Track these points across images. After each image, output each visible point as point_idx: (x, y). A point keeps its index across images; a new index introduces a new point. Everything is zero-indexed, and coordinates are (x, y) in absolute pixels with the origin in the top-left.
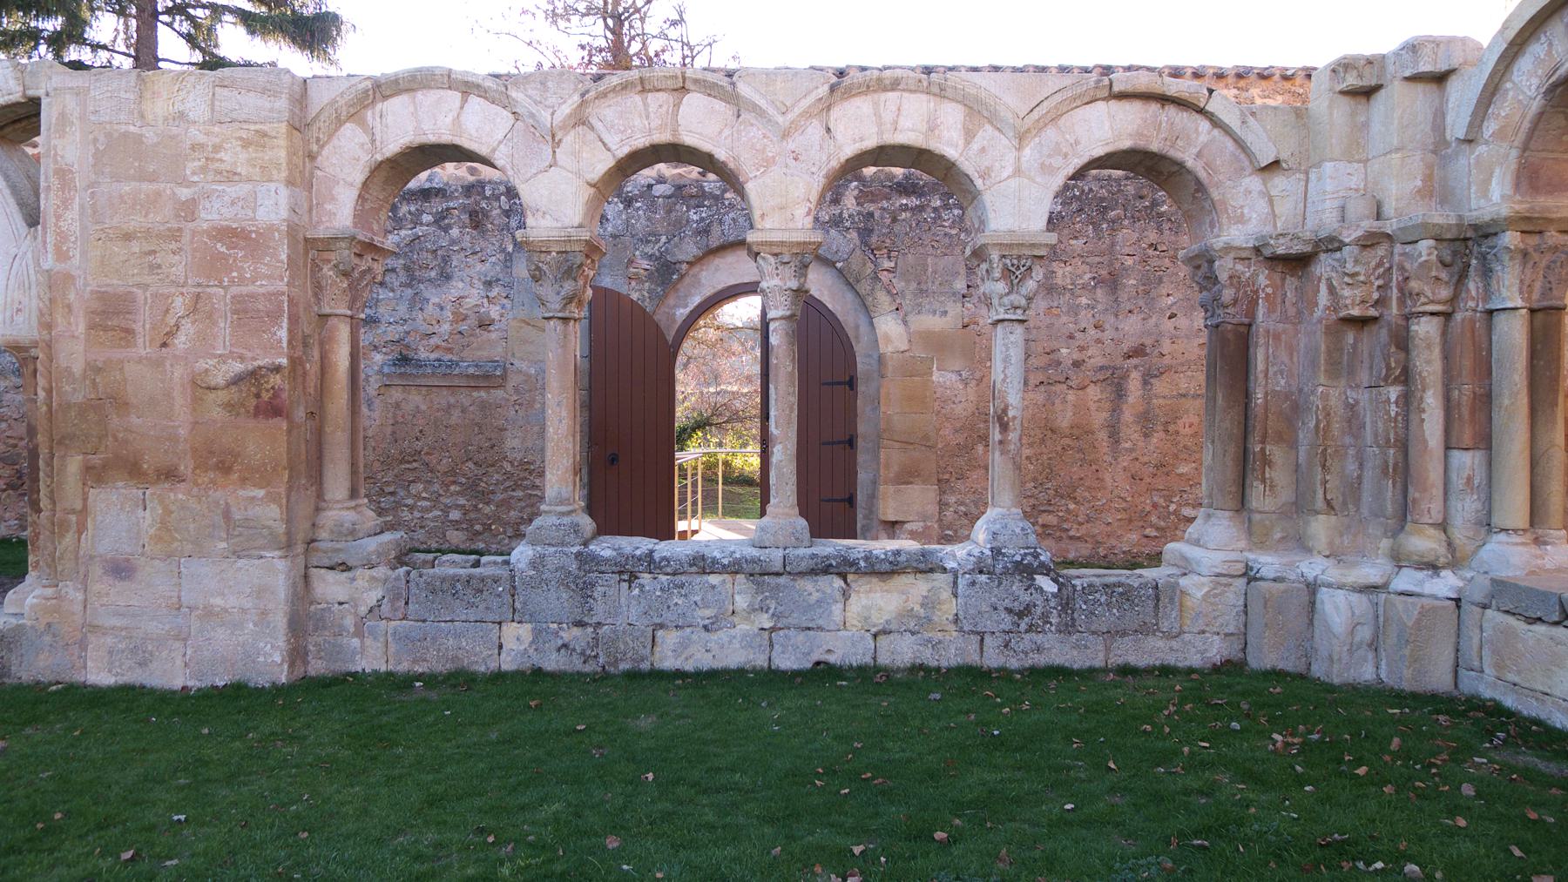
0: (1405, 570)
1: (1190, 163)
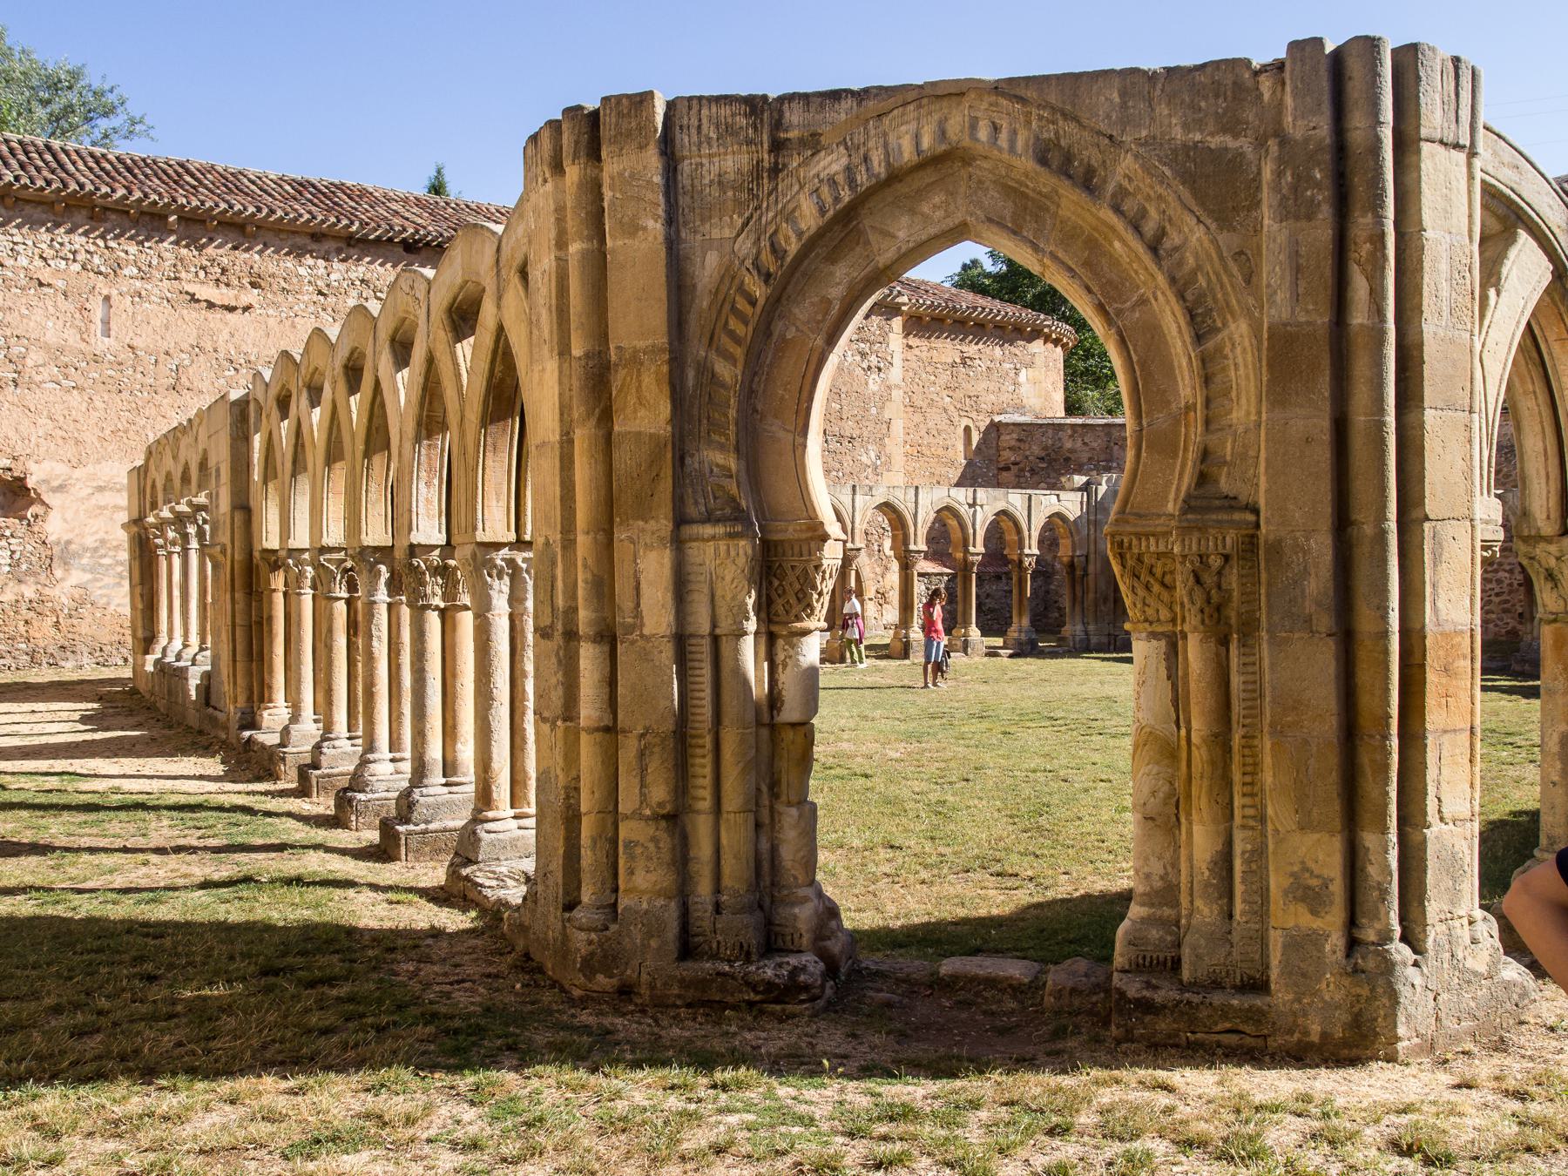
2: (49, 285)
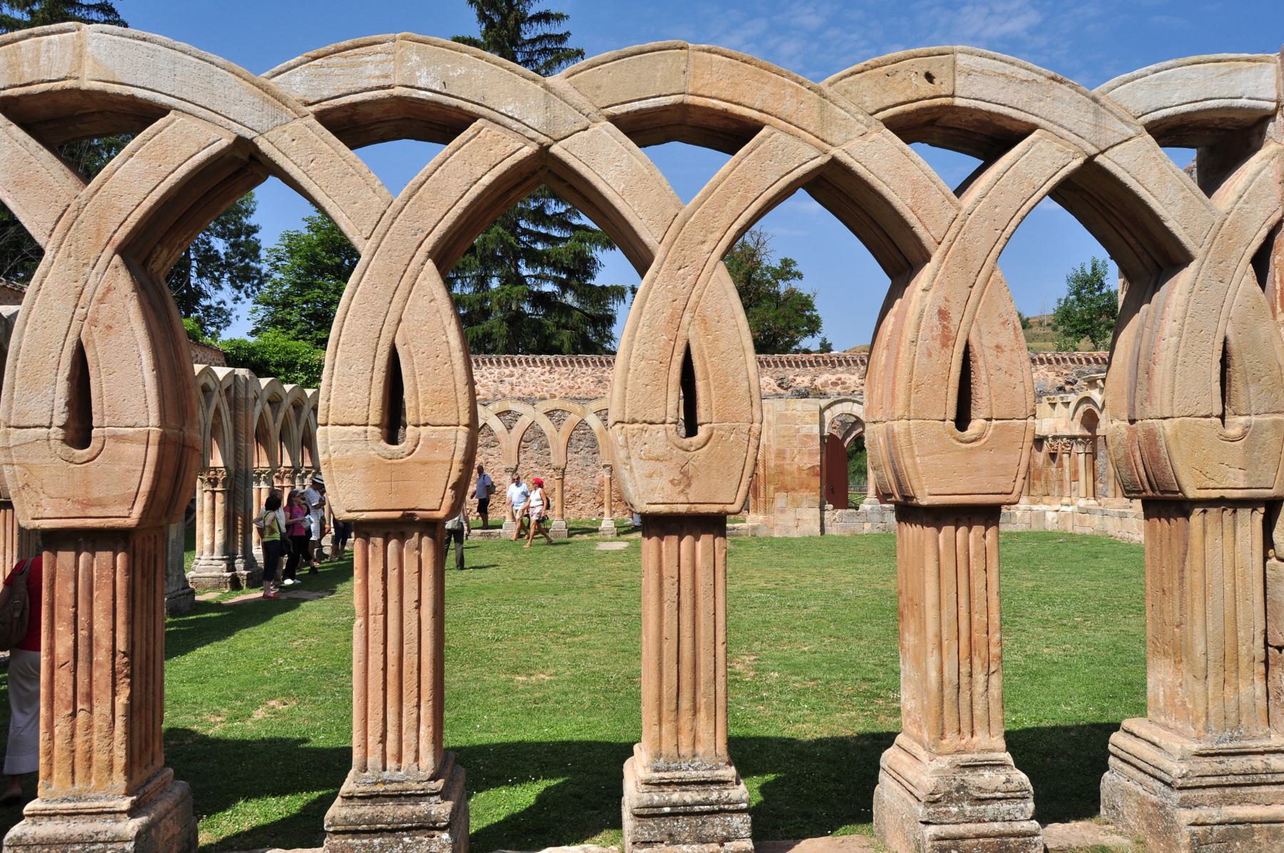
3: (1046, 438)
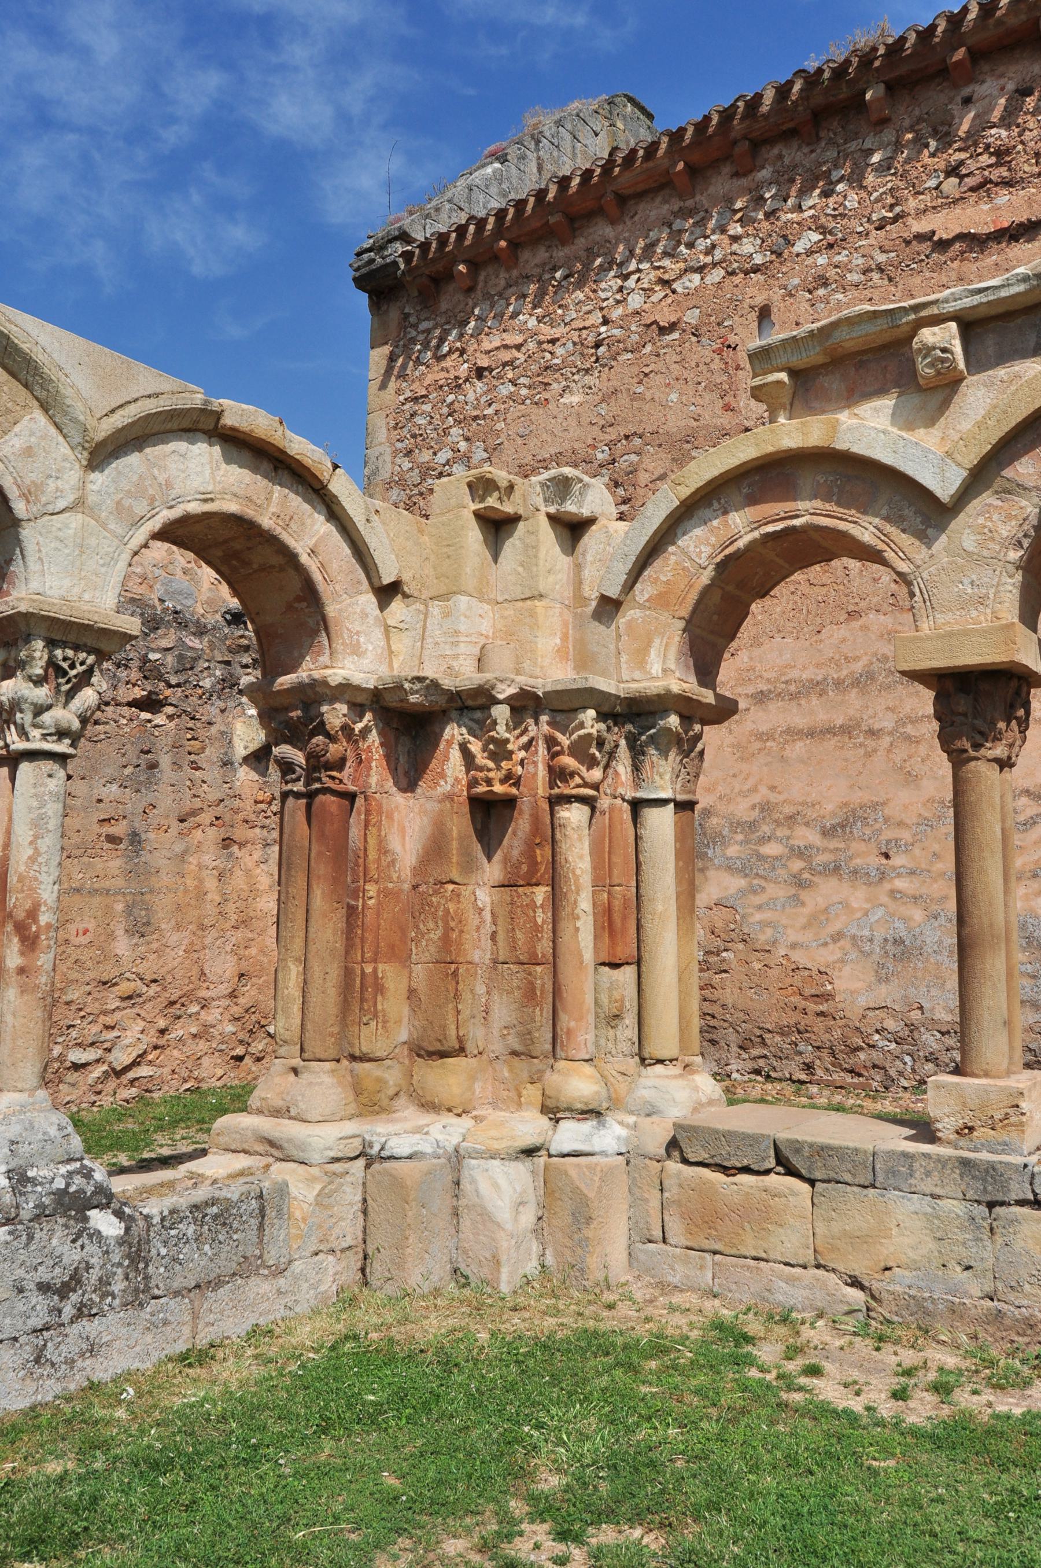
0: (563, 1124)
1: (304, 559)
2: (673, 327)
3: (472, 704)
